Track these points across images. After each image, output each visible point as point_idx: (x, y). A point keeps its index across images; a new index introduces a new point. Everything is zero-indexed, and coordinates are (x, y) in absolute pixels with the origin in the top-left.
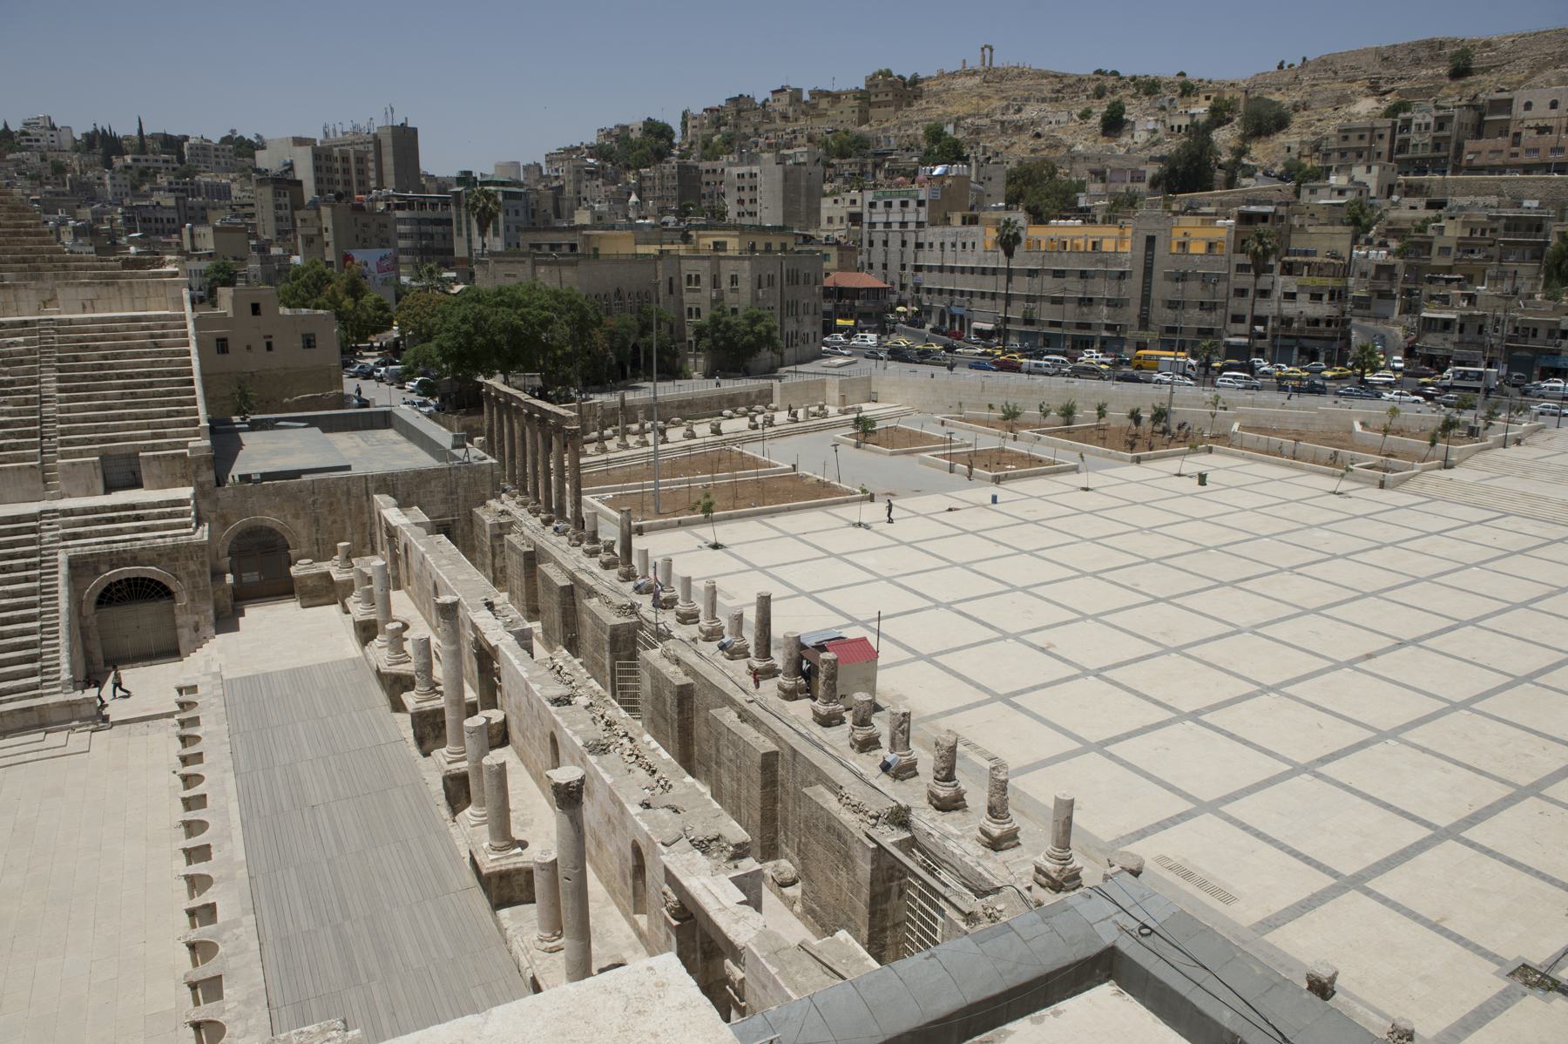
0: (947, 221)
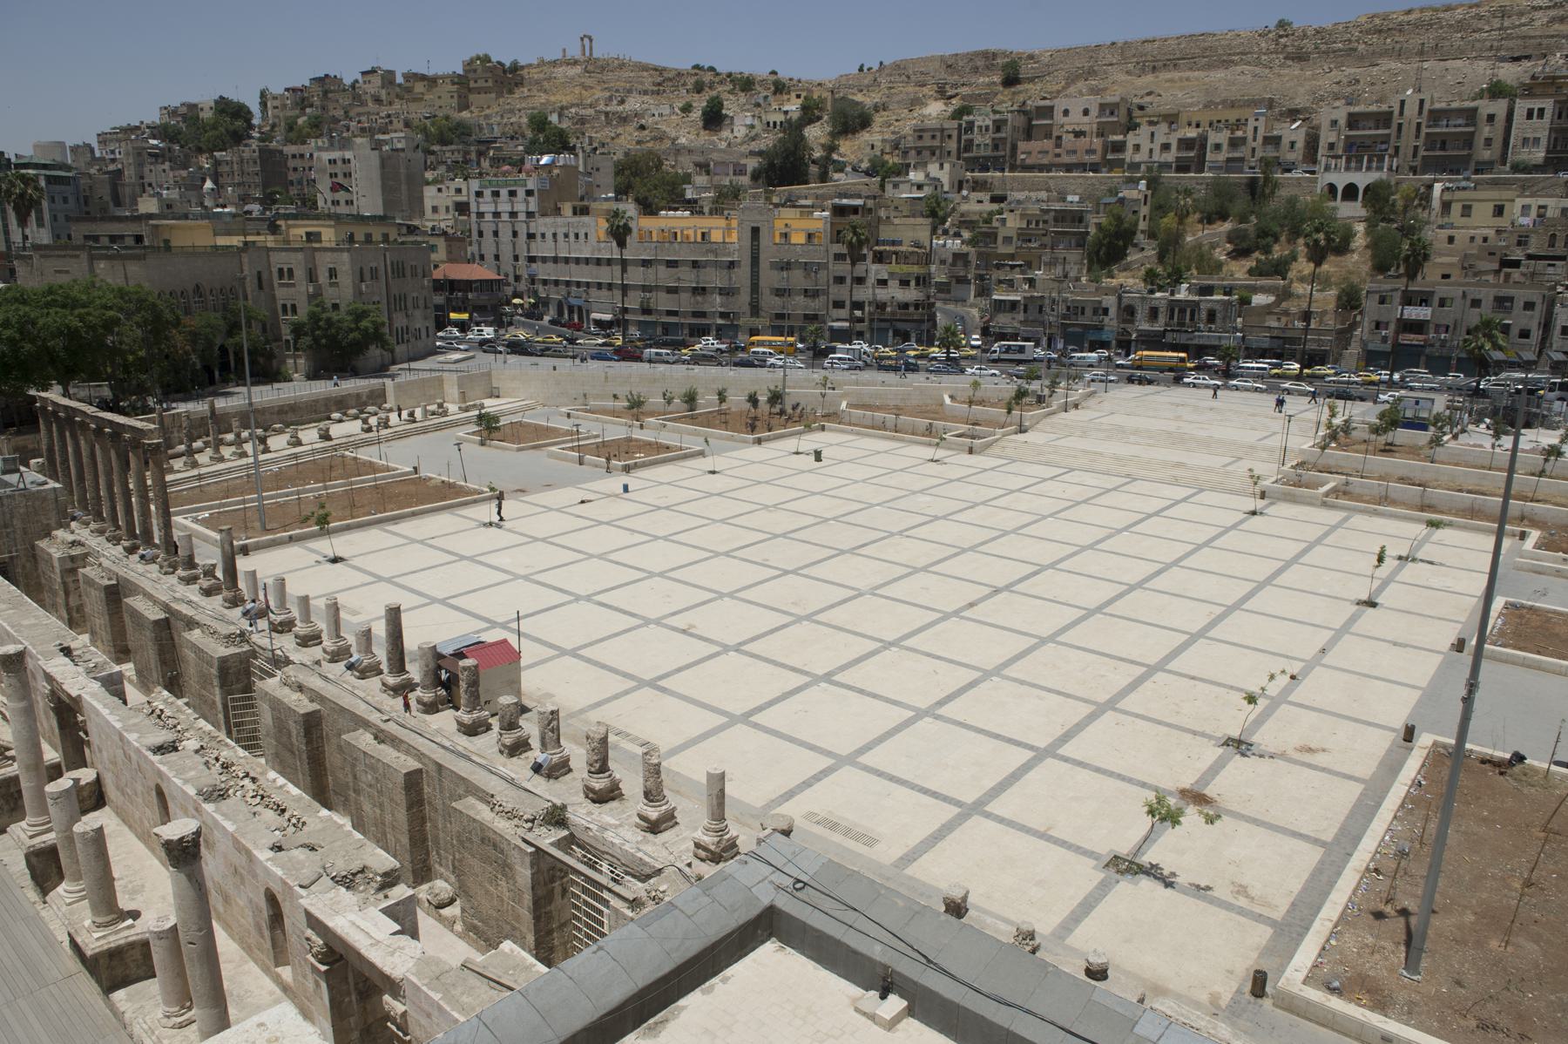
0: (557, 211)
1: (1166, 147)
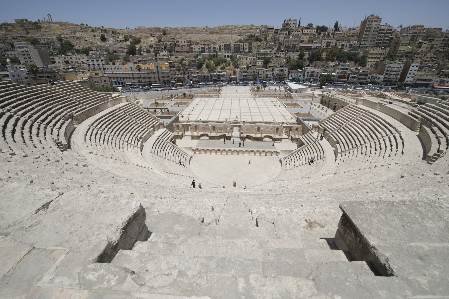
1: (199, 49)
